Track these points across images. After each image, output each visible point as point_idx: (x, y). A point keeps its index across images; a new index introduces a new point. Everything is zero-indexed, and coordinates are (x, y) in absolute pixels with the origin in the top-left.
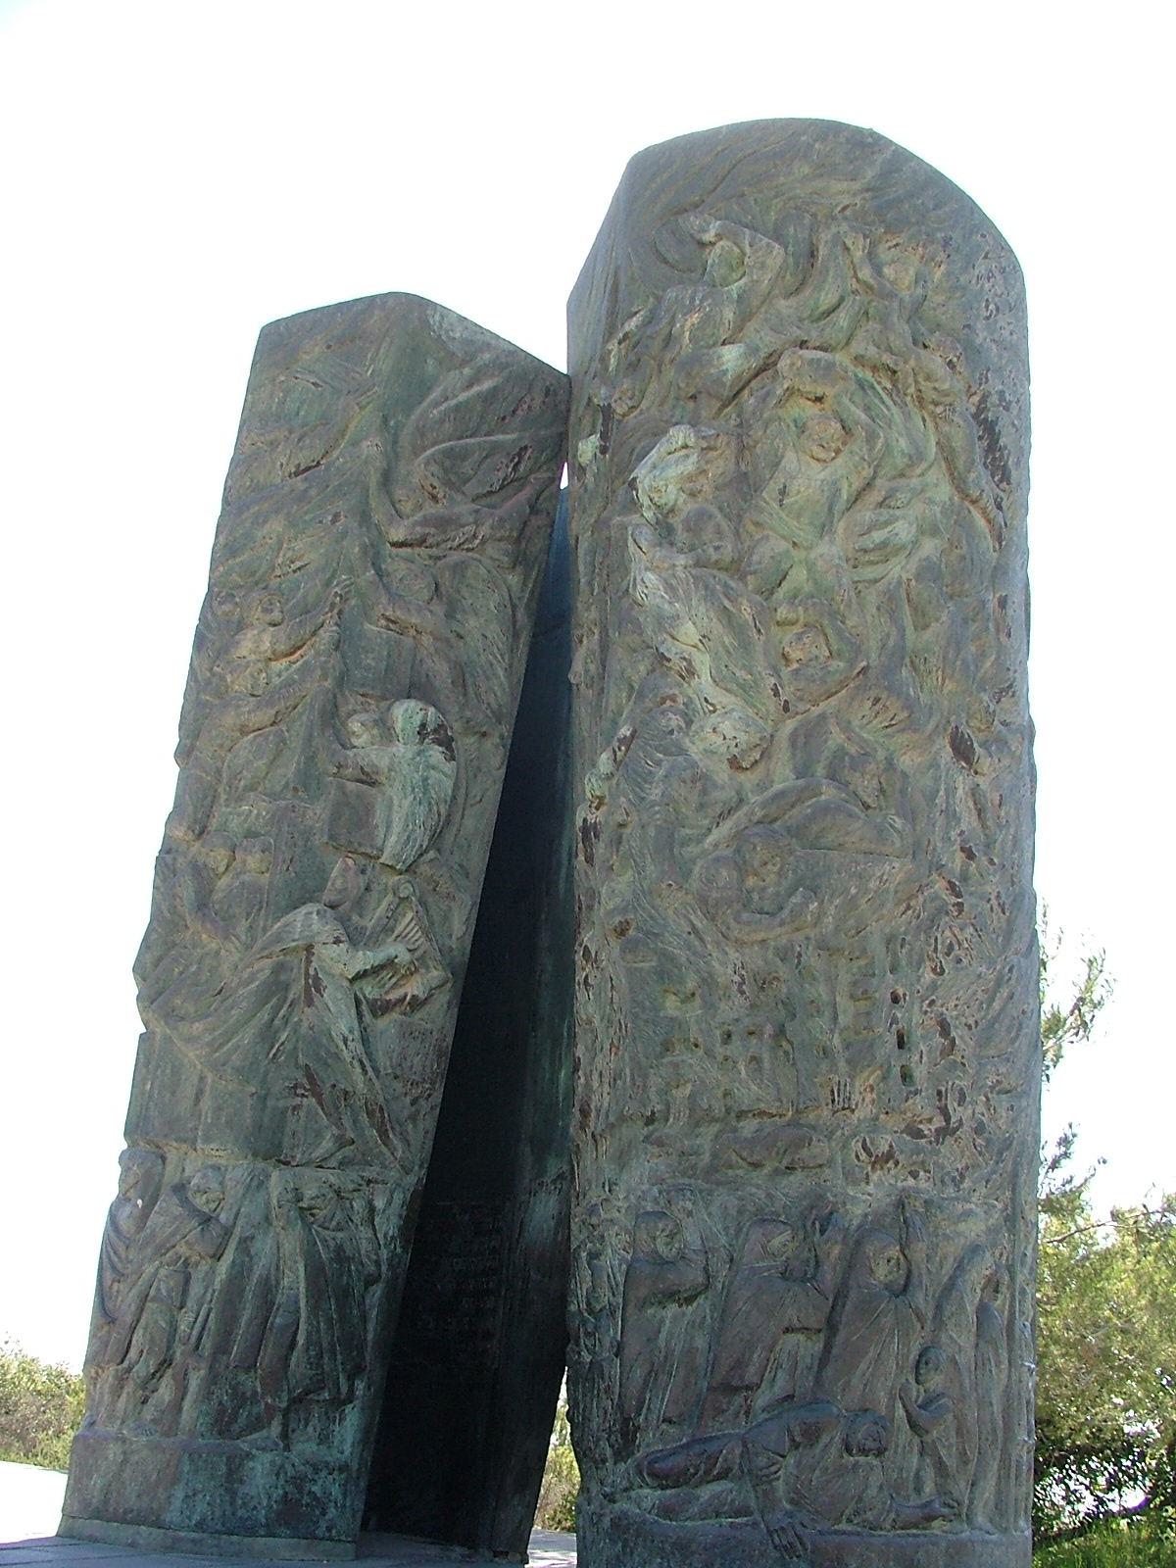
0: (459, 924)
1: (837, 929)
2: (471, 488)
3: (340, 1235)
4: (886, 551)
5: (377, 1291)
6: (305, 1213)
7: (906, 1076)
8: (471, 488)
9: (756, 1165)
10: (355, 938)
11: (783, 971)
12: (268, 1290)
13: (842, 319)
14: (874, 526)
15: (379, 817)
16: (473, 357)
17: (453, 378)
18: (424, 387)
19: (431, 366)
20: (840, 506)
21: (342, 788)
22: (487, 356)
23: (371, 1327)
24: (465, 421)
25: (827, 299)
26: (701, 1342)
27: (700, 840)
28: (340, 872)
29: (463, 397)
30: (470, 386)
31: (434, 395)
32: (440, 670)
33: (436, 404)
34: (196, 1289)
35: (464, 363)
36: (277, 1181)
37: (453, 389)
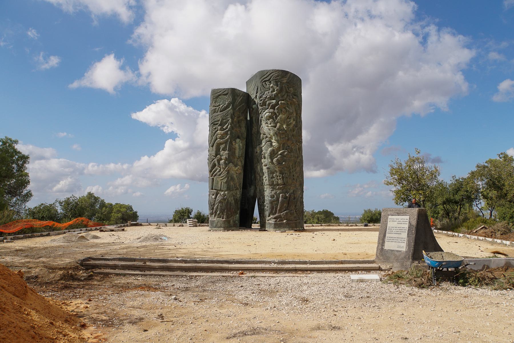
4: (291, 124)
5: (239, 203)
12: (230, 203)
13: (285, 96)
17: (238, 98)
18: (236, 100)
25: (284, 94)
36: (231, 192)
37: (239, 100)
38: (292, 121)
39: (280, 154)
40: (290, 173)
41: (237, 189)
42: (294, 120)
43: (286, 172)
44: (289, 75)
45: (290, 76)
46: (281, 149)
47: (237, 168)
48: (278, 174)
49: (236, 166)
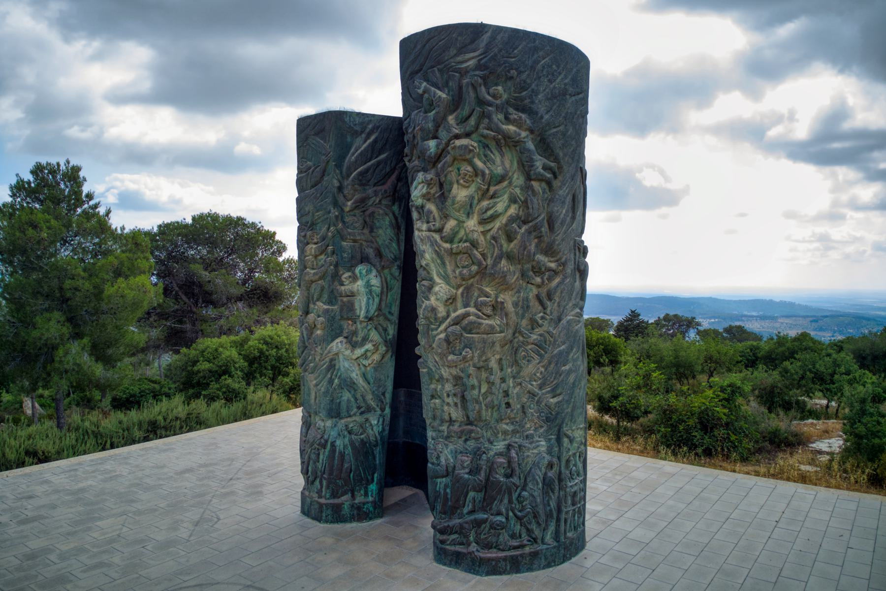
0: (392, 331)
1: (479, 361)
2: (372, 182)
3: (362, 436)
6: (350, 433)
7: (508, 405)
8: (372, 182)
9: (460, 437)
10: (354, 346)
11: (462, 375)
12: (342, 455)
13: (472, 121)
14: (488, 209)
15: (357, 306)
16: (365, 128)
17: (359, 140)
19: (349, 139)
20: (475, 201)
21: (342, 301)
22: (370, 126)
23: (377, 459)
24: (365, 157)
25: (466, 112)
26: (448, 490)
27: (436, 329)
28: (348, 326)
29: (362, 148)
30: (365, 141)
31: (352, 150)
32: (370, 252)
33: (353, 154)
34: (321, 457)
35: (362, 132)
37: (361, 145)
38: (500, 207)
39: (457, 322)
40: (491, 384)
41: (369, 409)
42: (513, 200)
43: (475, 382)
44: (486, 37)
45: (493, 38)
46: (459, 303)
47: (359, 352)
48: (448, 387)
49: (354, 346)
